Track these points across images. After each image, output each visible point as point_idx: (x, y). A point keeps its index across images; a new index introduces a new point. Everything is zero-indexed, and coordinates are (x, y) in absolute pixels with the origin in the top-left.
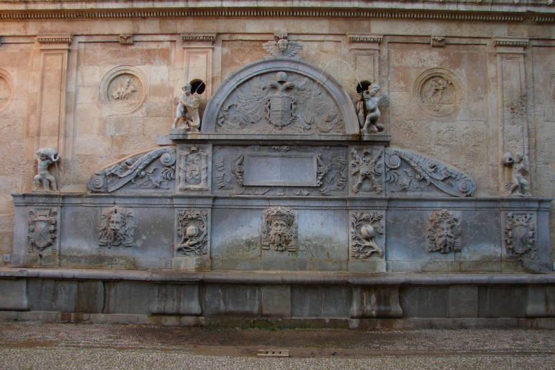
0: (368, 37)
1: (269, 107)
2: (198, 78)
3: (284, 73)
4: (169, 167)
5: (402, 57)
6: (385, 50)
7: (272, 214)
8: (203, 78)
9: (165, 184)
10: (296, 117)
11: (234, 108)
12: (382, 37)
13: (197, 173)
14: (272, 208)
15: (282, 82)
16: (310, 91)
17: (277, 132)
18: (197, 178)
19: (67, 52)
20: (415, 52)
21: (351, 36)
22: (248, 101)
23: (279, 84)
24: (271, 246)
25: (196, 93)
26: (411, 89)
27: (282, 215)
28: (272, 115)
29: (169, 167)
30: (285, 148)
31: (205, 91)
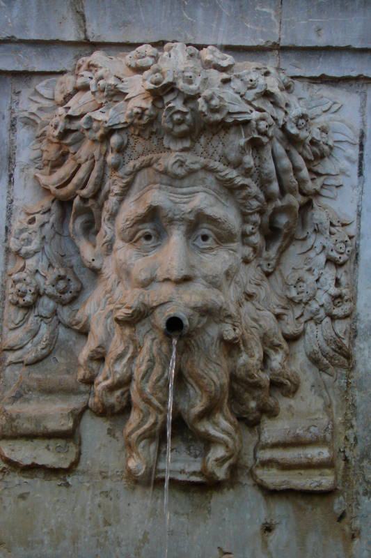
7: (109, 116)
14: (109, 66)
24: (94, 430)
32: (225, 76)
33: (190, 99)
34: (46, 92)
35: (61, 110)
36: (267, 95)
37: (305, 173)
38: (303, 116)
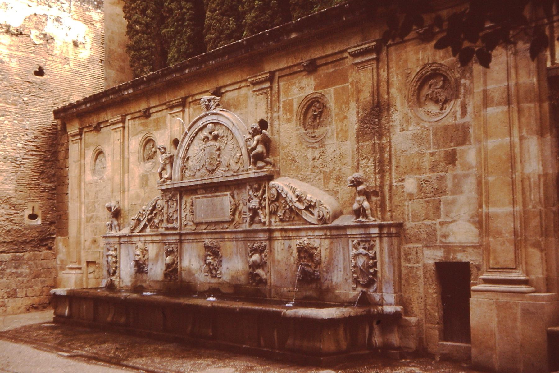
3: (211, 125)
6: (275, 86)
19: (122, 129)
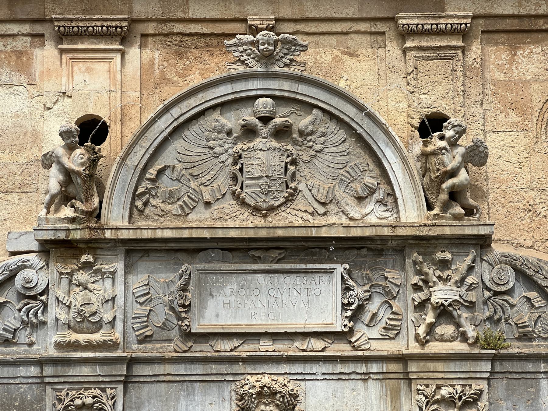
0: (442, 21)
1: (241, 170)
2: (92, 112)
3: (269, 100)
4: (34, 298)
5: (511, 61)
6: (476, 48)
8: (103, 114)
9: (23, 336)
10: (295, 189)
11: (168, 172)
12: (469, 20)
13: (94, 308)
15: (265, 120)
16: (323, 135)
17: (259, 221)
18: (92, 319)
20: (538, 49)
21: (404, 21)
22: (197, 159)
23: (259, 124)
25: (89, 144)
26: (532, 125)
27: (274, 394)
28: (248, 186)
29: (34, 298)
30: (275, 254)
31: (107, 139)
32: (276, 382)
33: (269, 388)
34: (238, 384)
35: (242, 389)
36: (285, 385)
37: (293, 400)
38: (292, 389)
